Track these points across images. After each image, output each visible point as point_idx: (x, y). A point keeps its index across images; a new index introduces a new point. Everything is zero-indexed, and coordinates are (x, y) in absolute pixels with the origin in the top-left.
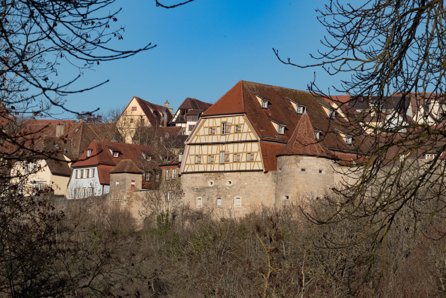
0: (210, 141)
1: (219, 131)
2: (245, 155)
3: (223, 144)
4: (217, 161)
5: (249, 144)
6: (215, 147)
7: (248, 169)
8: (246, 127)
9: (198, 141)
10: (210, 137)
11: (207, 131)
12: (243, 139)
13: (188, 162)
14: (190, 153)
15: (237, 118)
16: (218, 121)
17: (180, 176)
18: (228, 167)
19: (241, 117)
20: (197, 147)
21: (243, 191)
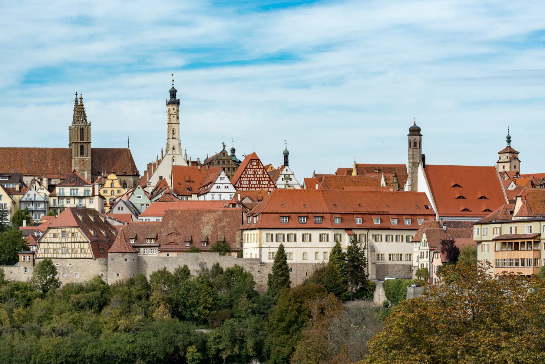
0: (55, 241)
1: (60, 235)
2: (79, 250)
3: (64, 243)
4: (60, 252)
5: (82, 244)
6: (58, 245)
7: (82, 257)
8: (79, 234)
9: (46, 241)
10: (54, 239)
11: (52, 235)
12: (78, 241)
13: (39, 252)
14: (41, 247)
15: (73, 229)
16: (60, 230)
17: (34, 260)
18: (68, 256)
19: (76, 229)
20: (46, 244)
21: (80, 269)
